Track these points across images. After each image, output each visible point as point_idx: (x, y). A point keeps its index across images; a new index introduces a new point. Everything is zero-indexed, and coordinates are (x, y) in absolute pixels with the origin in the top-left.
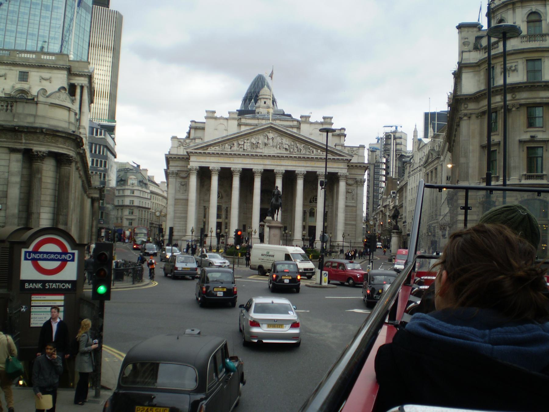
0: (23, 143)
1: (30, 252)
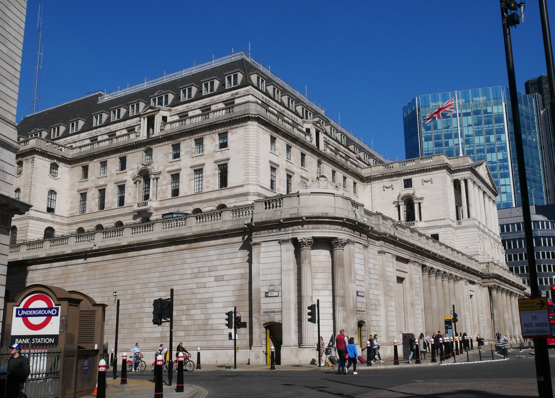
0: (289, 233)
1: (21, 310)
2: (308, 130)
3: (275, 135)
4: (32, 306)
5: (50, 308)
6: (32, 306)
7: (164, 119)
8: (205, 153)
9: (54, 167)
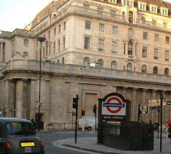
2: (124, 13)
3: (89, 20)
4: (111, 102)
5: (120, 104)
6: (111, 102)
7: (55, 15)
8: (61, 32)
9: (26, 41)
